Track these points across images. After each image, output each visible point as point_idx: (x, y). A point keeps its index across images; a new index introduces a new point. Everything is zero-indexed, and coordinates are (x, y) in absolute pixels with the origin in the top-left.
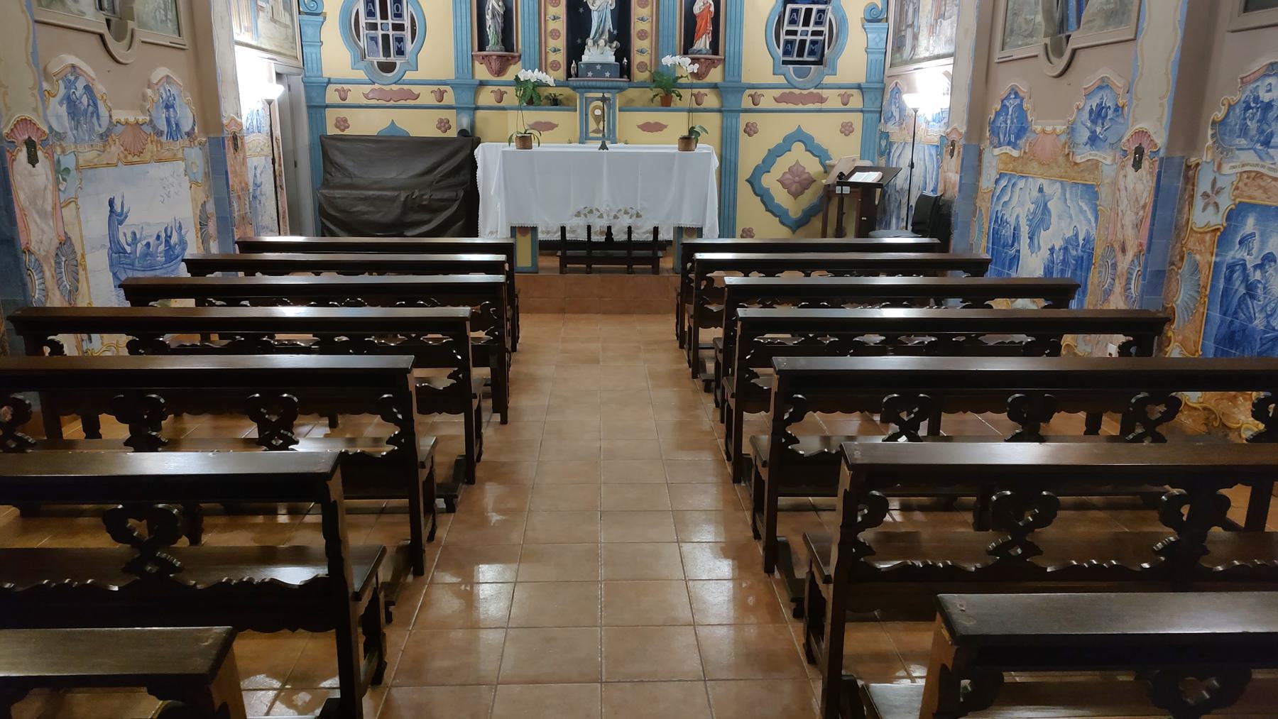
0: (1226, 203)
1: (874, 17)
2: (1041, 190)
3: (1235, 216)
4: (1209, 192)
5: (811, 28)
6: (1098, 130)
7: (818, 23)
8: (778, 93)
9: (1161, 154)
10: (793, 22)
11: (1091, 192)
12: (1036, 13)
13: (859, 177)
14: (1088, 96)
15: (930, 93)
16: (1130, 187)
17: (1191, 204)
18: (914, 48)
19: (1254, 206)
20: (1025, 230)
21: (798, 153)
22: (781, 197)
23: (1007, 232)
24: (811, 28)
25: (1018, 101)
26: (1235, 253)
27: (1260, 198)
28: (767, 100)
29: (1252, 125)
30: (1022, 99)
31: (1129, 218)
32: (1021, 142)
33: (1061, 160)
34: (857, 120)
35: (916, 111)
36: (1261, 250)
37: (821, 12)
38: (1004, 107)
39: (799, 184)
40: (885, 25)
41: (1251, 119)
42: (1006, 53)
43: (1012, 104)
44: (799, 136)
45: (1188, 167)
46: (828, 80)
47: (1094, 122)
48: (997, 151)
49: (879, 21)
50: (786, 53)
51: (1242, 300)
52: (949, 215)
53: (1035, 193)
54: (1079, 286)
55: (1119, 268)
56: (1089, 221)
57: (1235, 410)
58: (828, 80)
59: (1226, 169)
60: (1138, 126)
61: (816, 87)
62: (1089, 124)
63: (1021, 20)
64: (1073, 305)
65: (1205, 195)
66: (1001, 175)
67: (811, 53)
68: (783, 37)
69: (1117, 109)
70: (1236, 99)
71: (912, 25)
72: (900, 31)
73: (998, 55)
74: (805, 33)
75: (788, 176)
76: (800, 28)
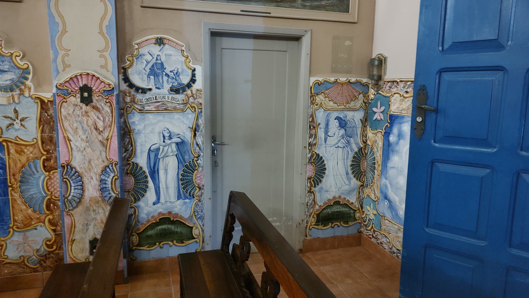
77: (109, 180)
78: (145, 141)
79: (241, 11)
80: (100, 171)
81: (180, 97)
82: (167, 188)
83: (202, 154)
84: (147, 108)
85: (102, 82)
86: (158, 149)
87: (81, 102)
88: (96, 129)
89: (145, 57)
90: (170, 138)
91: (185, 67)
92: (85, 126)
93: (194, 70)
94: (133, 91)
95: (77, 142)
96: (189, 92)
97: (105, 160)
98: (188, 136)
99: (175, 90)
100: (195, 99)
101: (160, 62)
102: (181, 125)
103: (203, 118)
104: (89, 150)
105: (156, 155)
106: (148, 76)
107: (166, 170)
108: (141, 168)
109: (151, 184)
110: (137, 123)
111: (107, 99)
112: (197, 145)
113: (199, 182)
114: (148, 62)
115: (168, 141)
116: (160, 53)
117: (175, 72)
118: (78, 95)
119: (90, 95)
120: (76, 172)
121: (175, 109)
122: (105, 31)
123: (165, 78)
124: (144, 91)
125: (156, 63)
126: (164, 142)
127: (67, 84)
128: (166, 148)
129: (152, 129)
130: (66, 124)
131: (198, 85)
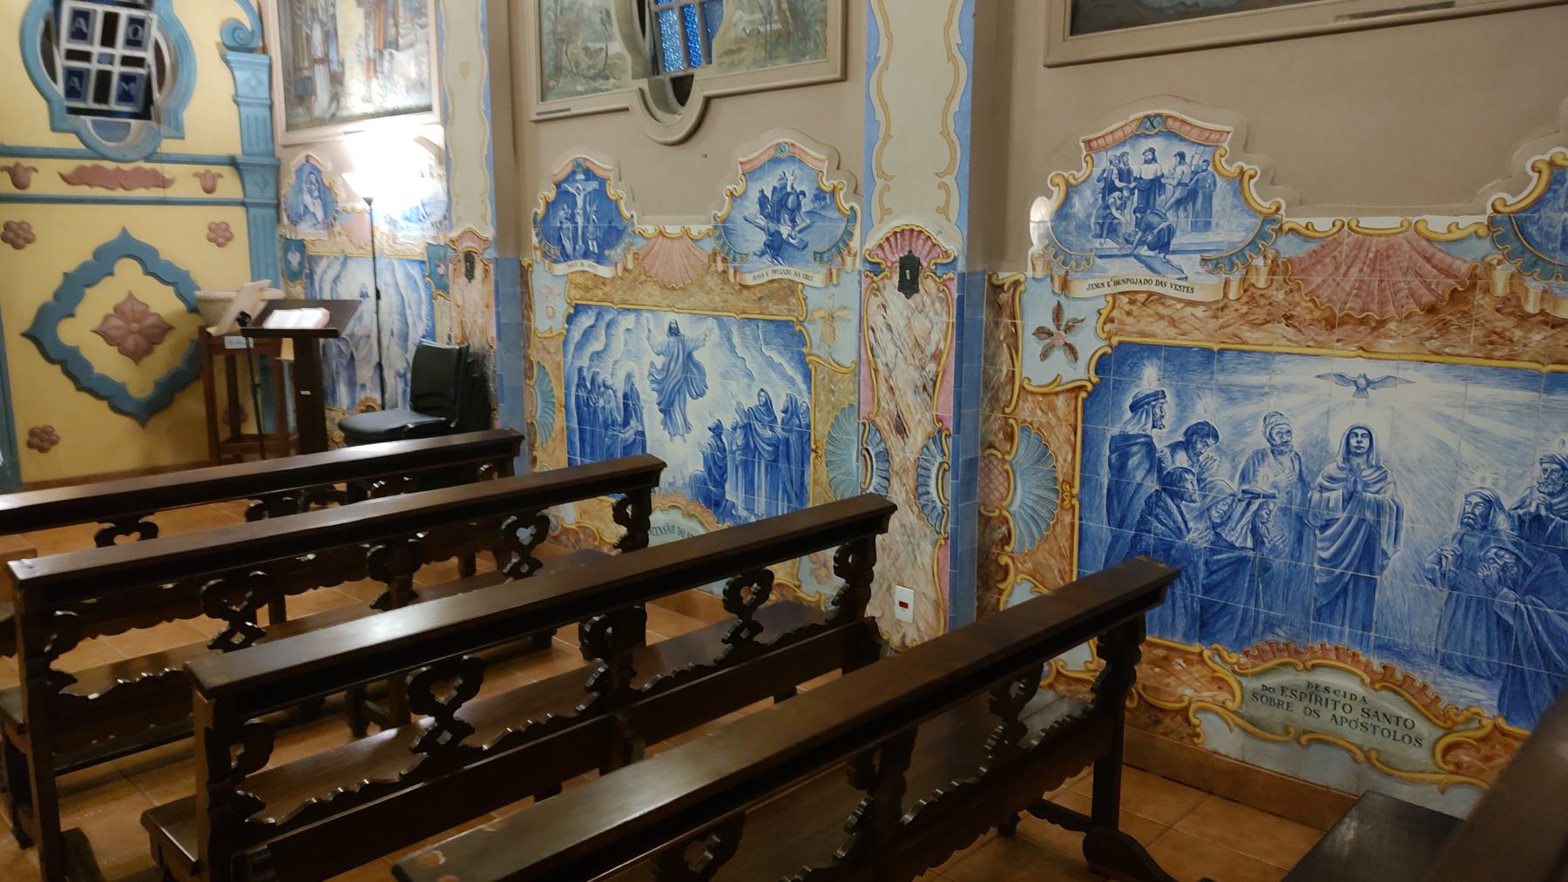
0: (1090, 344)
1: (239, 43)
2: (674, 331)
3: (1116, 363)
4: (1052, 327)
5: (120, 50)
6: (785, 230)
7: (133, 42)
8: (69, 166)
10: (78, 34)
11: (790, 335)
12: (609, 38)
13: (281, 320)
14: (751, 174)
15: (393, 168)
16: (899, 323)
17: (1014, 348)
18: (336, 97)
19: (1153, 350)
20: (649, 399)
21: (128, 278)
22: (107, 361)
23: (611, 404)
24: (120, 50)
25: (593, 185)
26: (1126, 423)
27: (1162, 334)
28: (46, 178)
29: (1126, 219)
30: (603, 182)
31: (906, 376)
32: (614, 253)
33: (712, 281)
34: (236, 219)
35: (369, 202)
36: (1180, 419)
37: (137, 23)
38: (564, 196)
39: (136, 335)
40: (263, 59)
41: (1121, 208)
42: (554, 104)
43: (581, 190)
44: (126, 248)
45: (998, 288)
46: (169, 146)
47: (774, 217)
48: (561, 269)
49: (251, 51)
50: (71, 92)
51: (1153, 503)
52: (483, 379)
53: (662, 338)
54: (522, 438)
55: (897, 461)
56: (792, 381)
57: (1171, 680)
58: (169, 146)
59: (1080, 288)
61: (148, 159)
62: (762, 221)
63: (576, 49)
64: (520, 465)
65: (1041, 332)
66: (578, 309)
67: (125, 97)
68: (60, 63)
69: (819, 196)
70: (1081, 175)
71: (325, 60)
72: (297, 69)
73: (533, 107)
74: (105, 58)
75: (116, 322)
76: (96, 49)
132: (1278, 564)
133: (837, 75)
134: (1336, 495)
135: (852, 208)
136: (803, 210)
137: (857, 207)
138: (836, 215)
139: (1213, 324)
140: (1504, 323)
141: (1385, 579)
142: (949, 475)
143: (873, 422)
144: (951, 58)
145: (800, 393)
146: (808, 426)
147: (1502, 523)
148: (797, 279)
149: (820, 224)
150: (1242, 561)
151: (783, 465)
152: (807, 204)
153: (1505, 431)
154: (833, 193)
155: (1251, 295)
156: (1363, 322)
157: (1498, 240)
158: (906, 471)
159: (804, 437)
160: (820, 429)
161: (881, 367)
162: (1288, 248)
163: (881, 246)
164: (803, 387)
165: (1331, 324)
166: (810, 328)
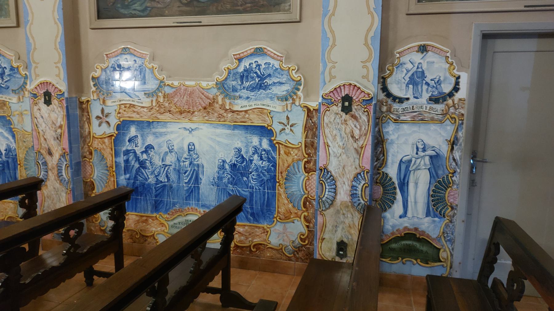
0: (114, 121)
3: (123, 126)
4: (101, 116)
9: (66, 95)
16: (46, 115)
17: (89, 123)
19: (133, 122)
26: (127, 146)
27: (136, 117)
31: (50, 134)
36: (143, 144)
45: (82, 103)
51: (138, 170)
55: (50, 165)
56: (7, 138)
57: (148, 226)
59: (109, 102)
60: (42, 79)
65: (98, 117)
70: (106, 65)
77: (360, 187)
78: (398, 152)
79: (525, 6)
80: (352, 177)
81: (440, 107)
82: (416, 202)
83: (458, 170)
84: (402, 118)
85: (362, 92)
86: (410, 161)
87: (342, 111)
88: (353, 137)
89: (405, 66)
90: (424, 150)
91: (448, 75)
92: (343, 134)
93: (459, 77)
94: (390, 101)
95: (335, 149)
96: (450, 102)
97: (358, 167)
98: (444, 149)
99: (434, 100)
100: (456, 109)
101: (420, 70)
102: (437, 137)
103: (464, 130)
104: (344, 156)
105: (407, 167)
106: (407, 85)
107: (416, 184)
108: (391, 179)
109: (399, 196)
110: (391, 132)
111: (365, 108)
112: (454, 160)
113: (452, 200)
114: (408, 71)
115: (421, 154)
116: (421, 61)
117: (436, 80)
118: (340, 105)
119: (350, 105)
120: (331, 176)
121: (432, 119)
122: (369, 42)
123: (425, 87)
124: (401, 100)
125: (416, 72)
126: (417, 154)
127: (331, 94)
128: (418, 161)
129: (406, 139)
130: (327, 131)
131: (462, 94)
132: (174, 185)
133: (15, 25)
134: (187, 163)
135: (26, 74)
136: (6, 74)
137: (27, 73)
138: (20, 76)
139: (150, 114)
140: (222, 112)
141: (201, 186)
142: (69, 168)
143: (39, 152)
144: (56, 23)
145: (11, 143)
146: (16, 155)
147: (227, 167)
148: (6, 100)
149: (13, 79)
150: (165, 186)
151: (7, 171)
152: (7, 72)
153: (226, 141)
154: (18, 68)
155: (159, 105)
156: (189, 112)
157: (219, 89)
158: (53, 168)
159: (15, 159)
160: (21, 156)
161: (40, 131)
162: (167, 90)
163: (36, 88)
164: (13, 141)
165: (181, 113)
166: (13, 118)
